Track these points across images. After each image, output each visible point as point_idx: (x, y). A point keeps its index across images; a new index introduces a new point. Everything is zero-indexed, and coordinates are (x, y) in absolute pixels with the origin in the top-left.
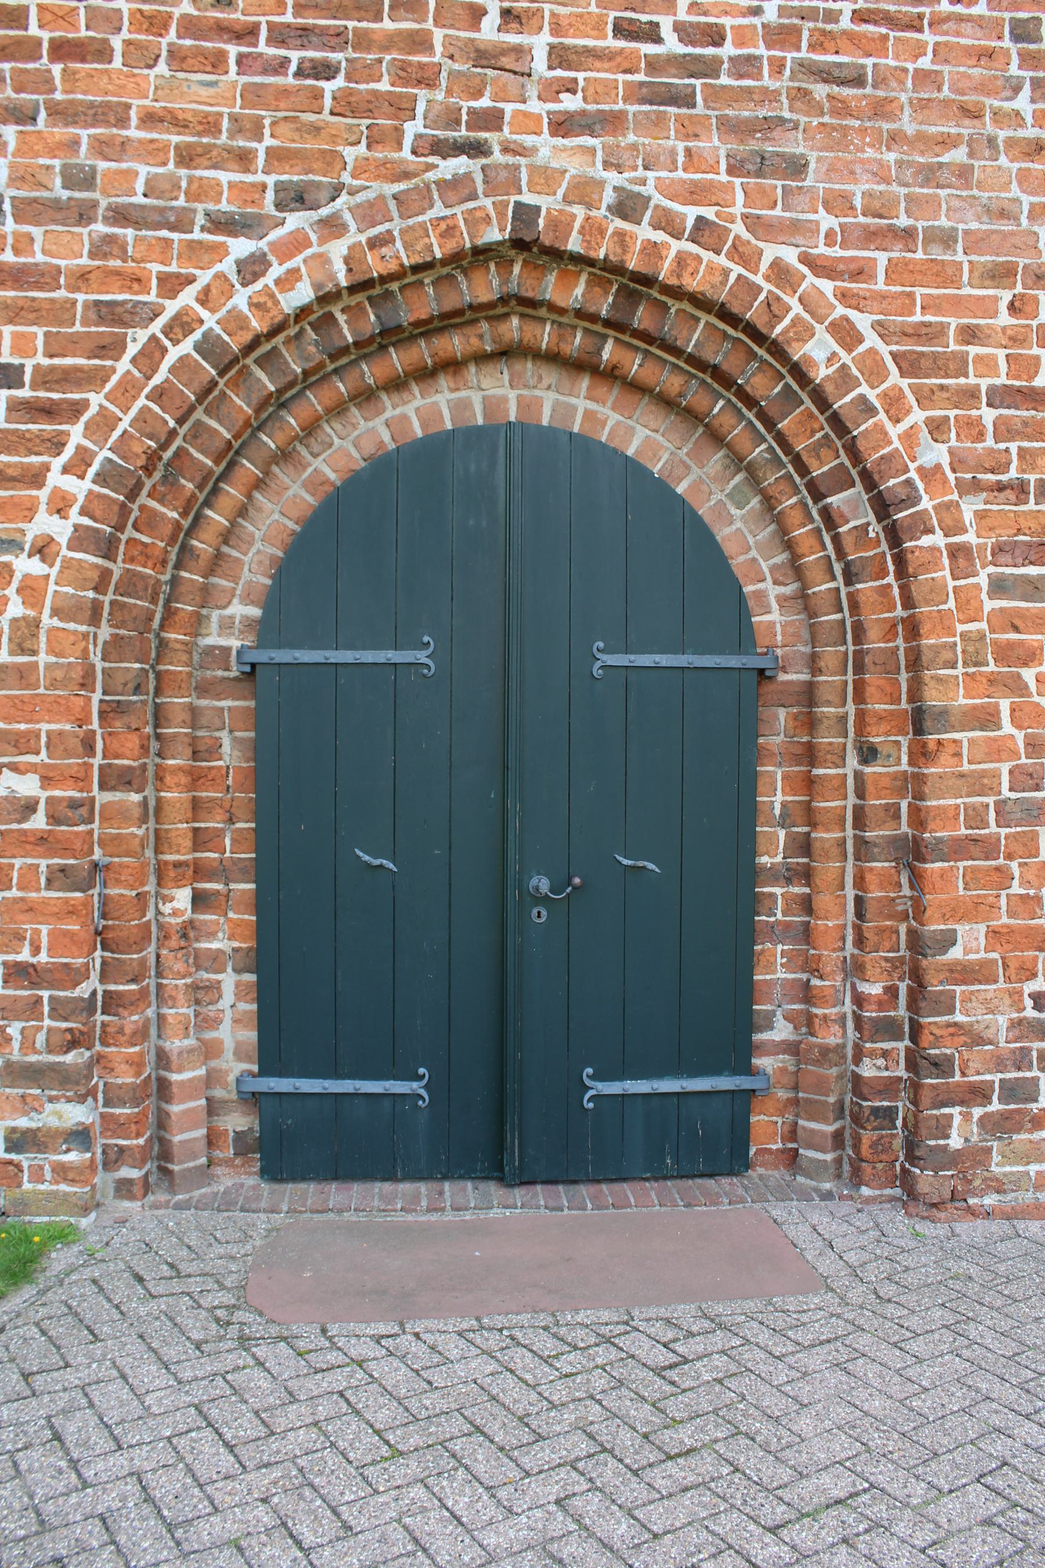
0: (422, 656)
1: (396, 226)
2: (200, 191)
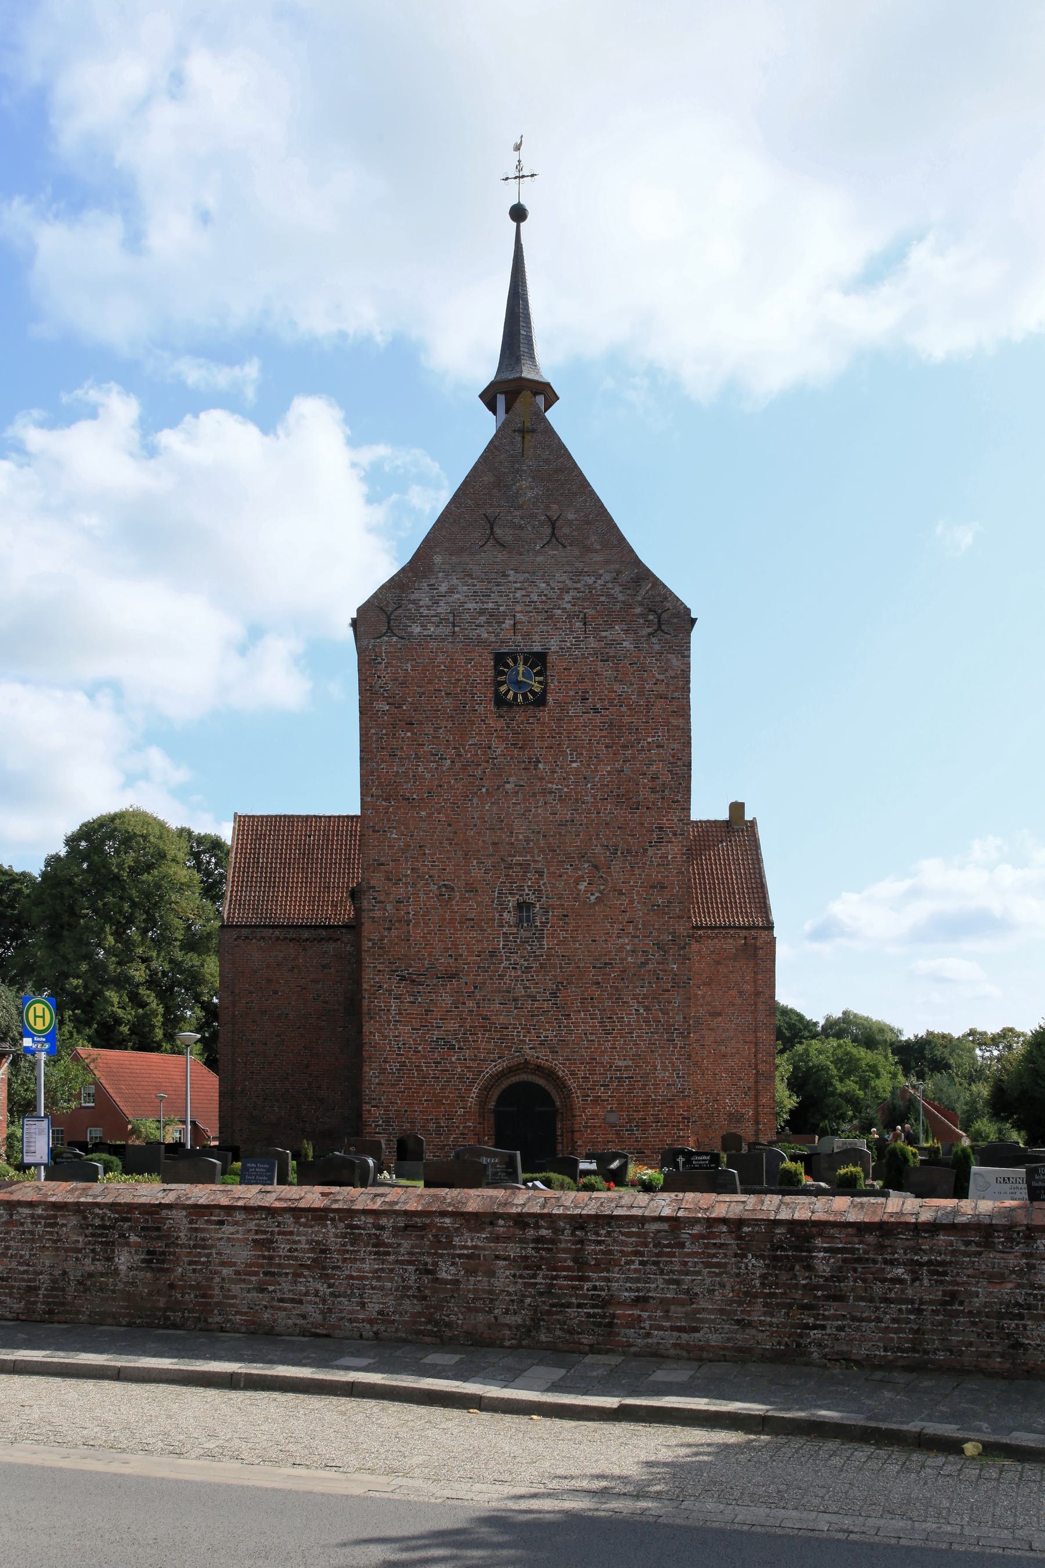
2: (489, 1057)
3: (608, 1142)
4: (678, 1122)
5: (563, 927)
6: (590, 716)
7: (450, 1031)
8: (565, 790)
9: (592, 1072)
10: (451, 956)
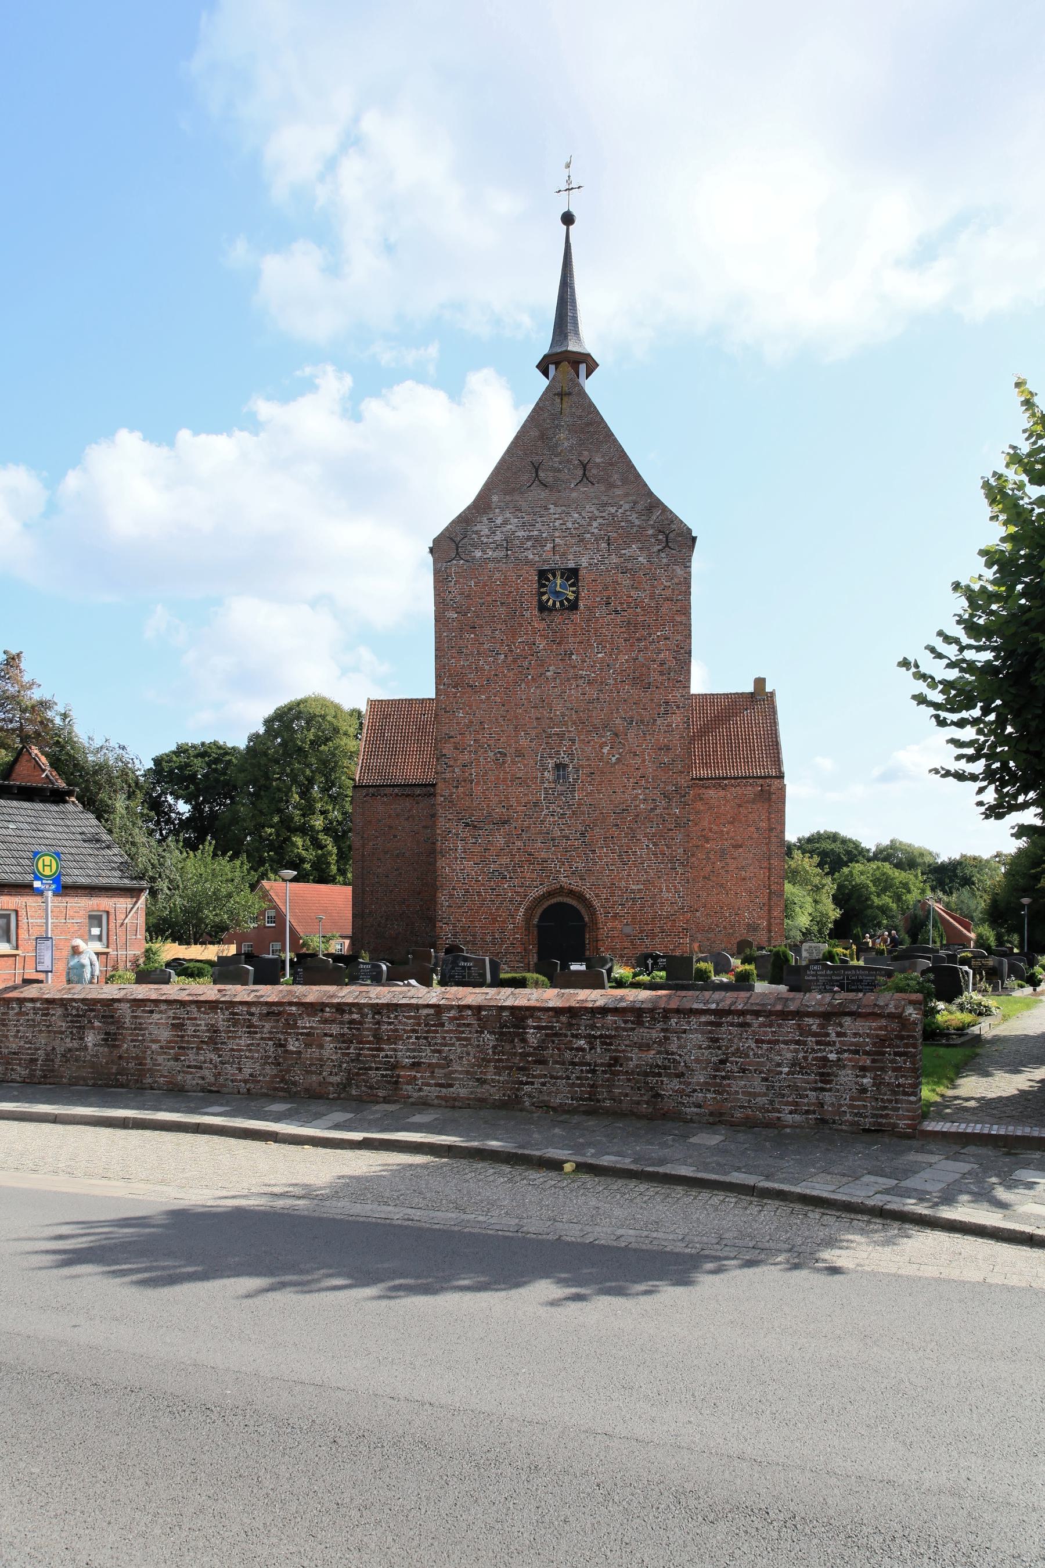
6: (612, 617)
8: (593, 675)
9: (612, 894)
10: (504, 806)
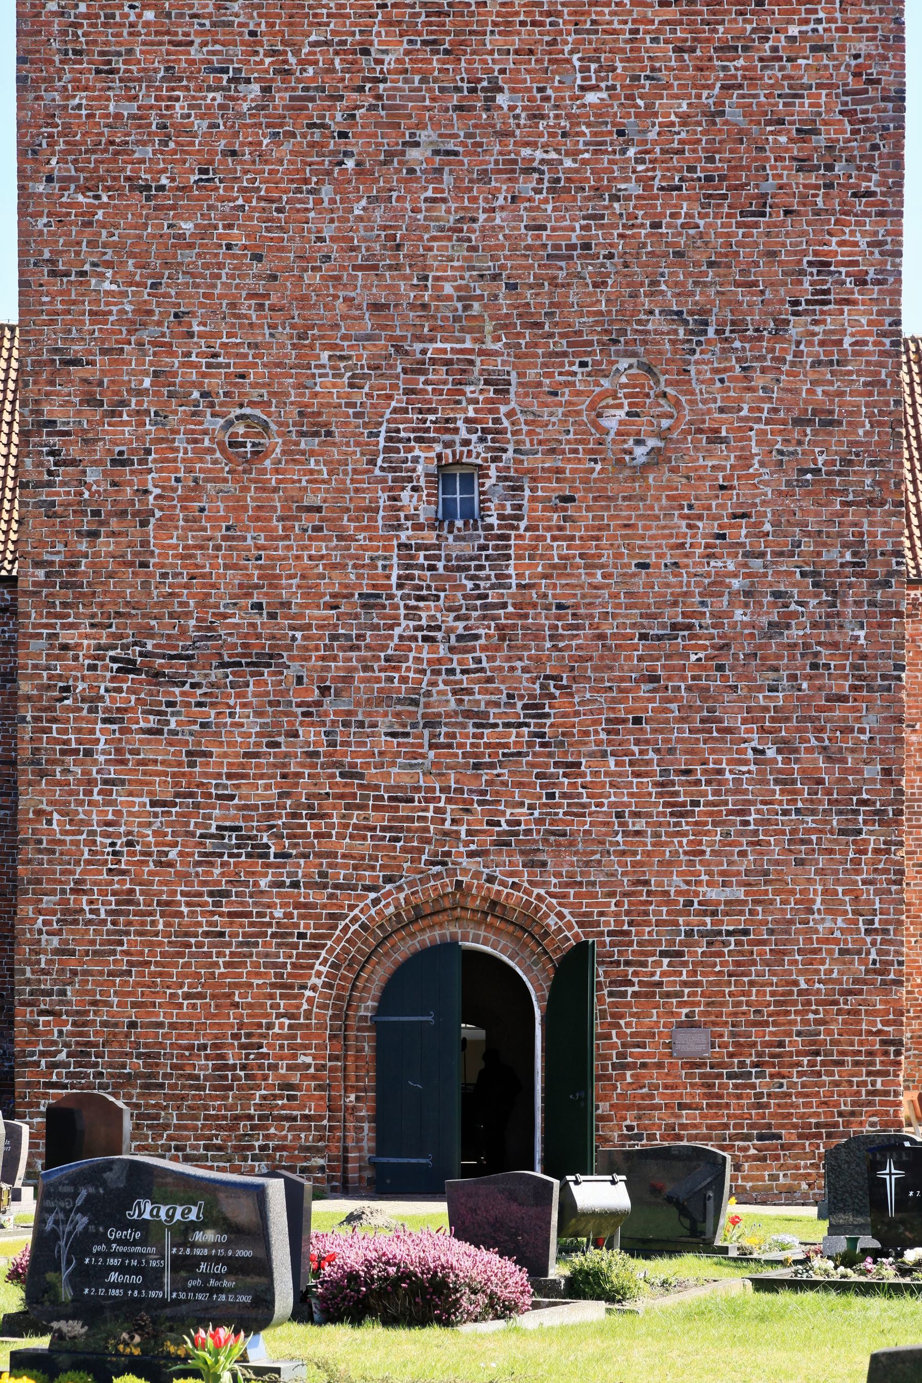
0: (430, 1018)
1: (419, 888)
2: (360, 878)
3: (682, 1106)
4: (870, 1053)
5: (561, 528)
7: (256, 807)
8: (568, 163)
9: (639, 917)
10: (258, 606)
